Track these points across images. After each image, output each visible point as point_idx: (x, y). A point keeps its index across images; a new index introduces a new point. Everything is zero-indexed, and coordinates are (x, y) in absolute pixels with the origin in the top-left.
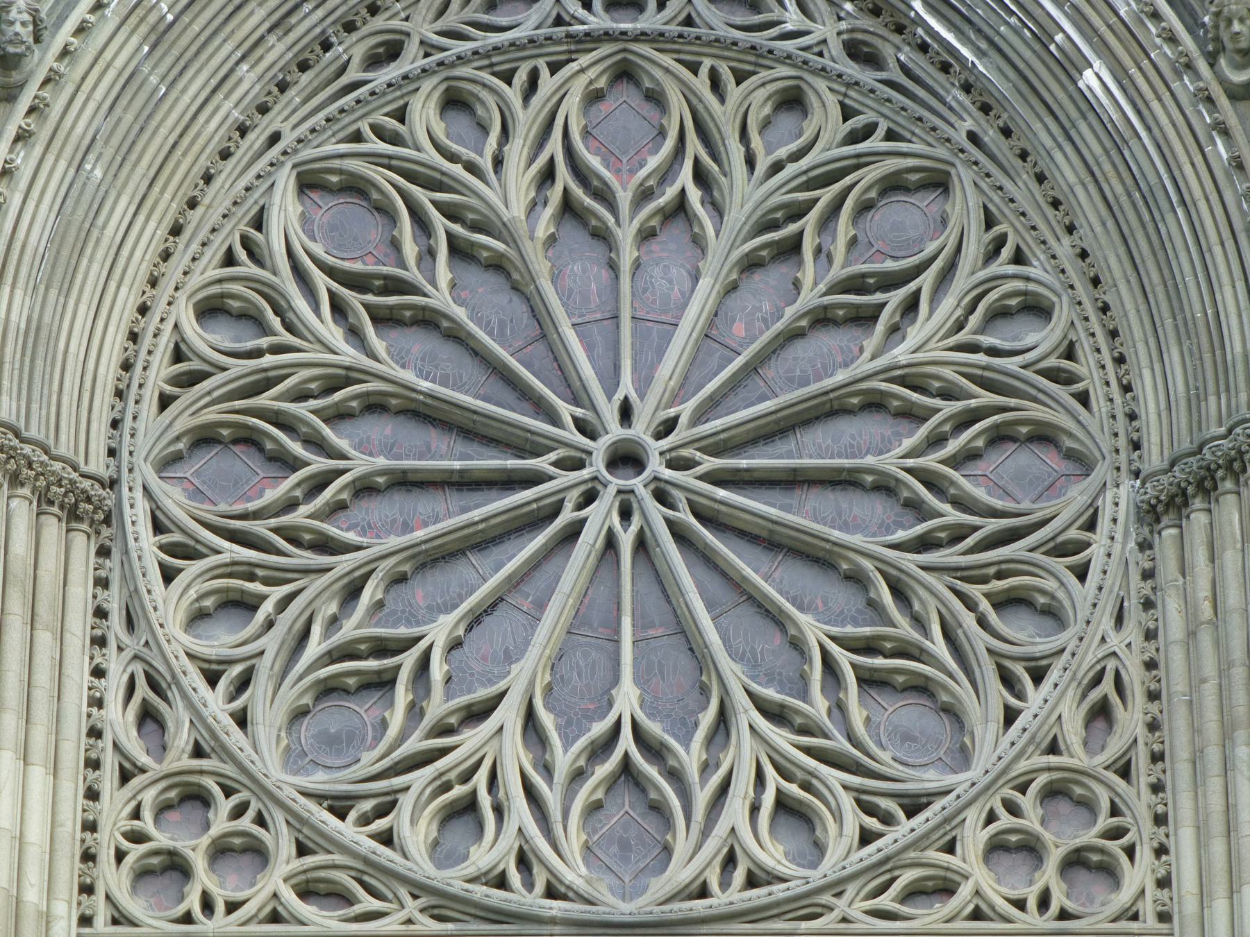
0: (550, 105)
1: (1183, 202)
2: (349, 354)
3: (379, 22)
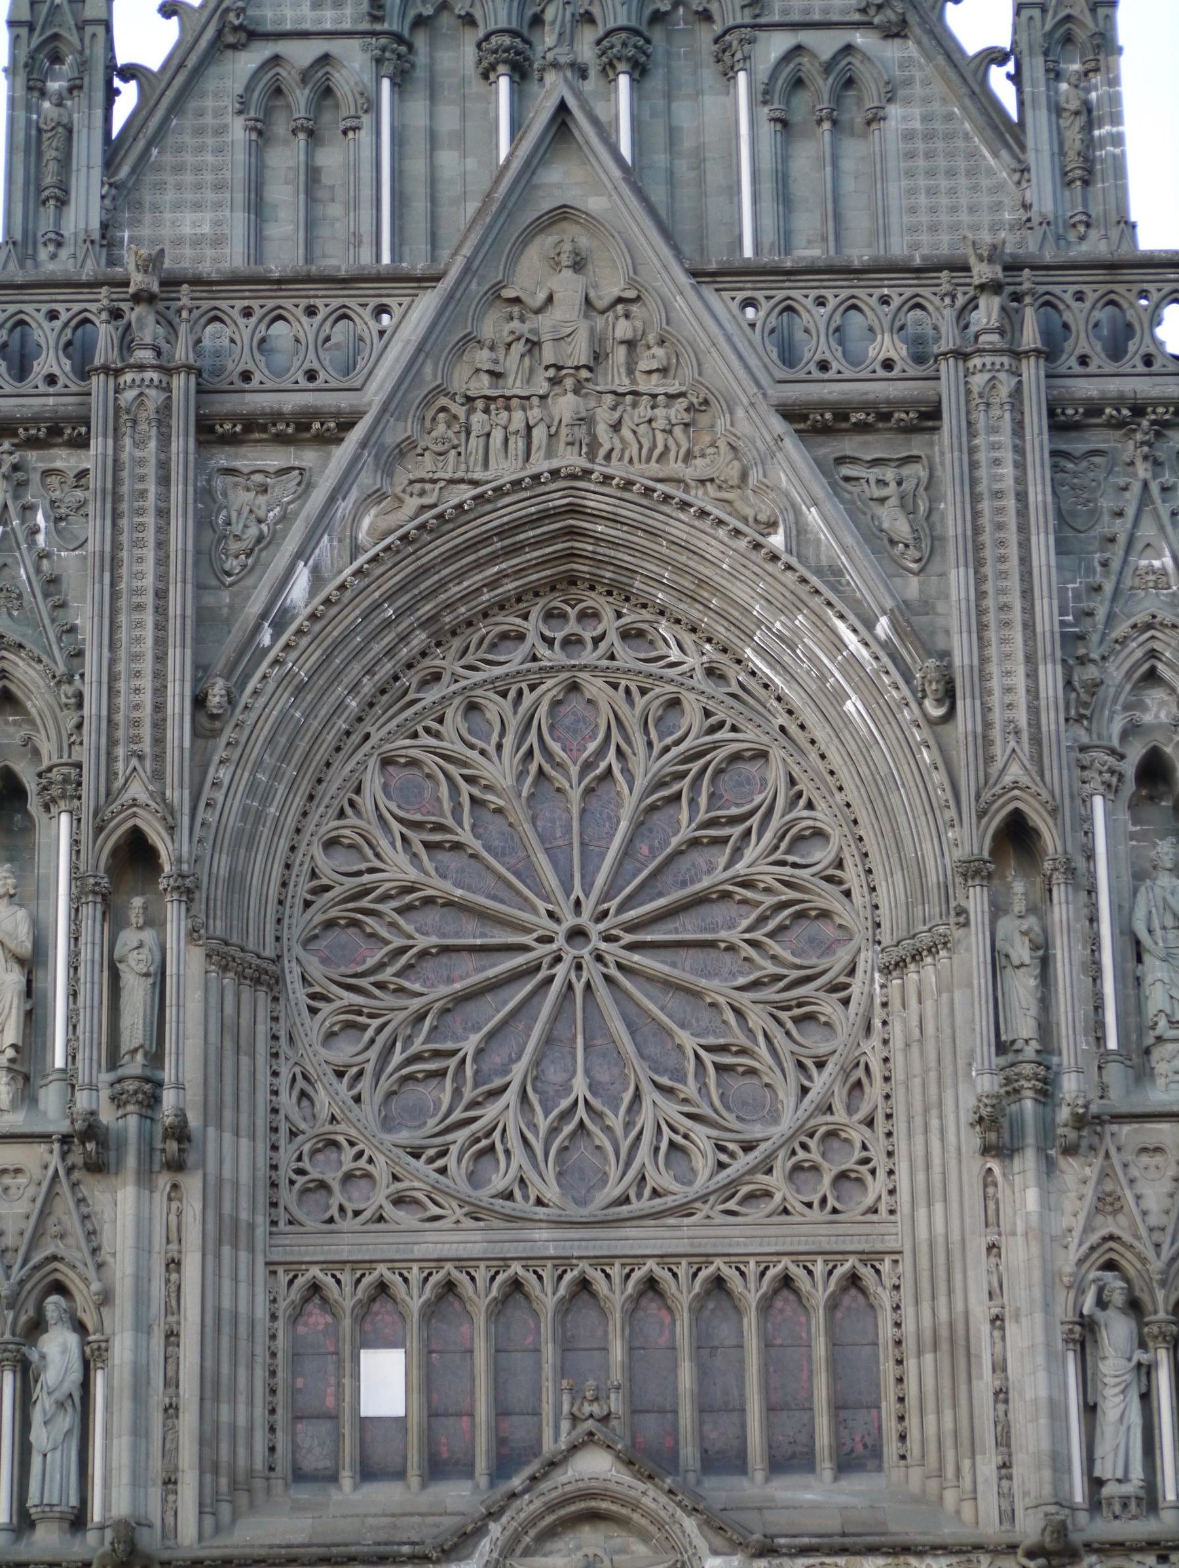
2: (413, 874)
3: (427, 662)
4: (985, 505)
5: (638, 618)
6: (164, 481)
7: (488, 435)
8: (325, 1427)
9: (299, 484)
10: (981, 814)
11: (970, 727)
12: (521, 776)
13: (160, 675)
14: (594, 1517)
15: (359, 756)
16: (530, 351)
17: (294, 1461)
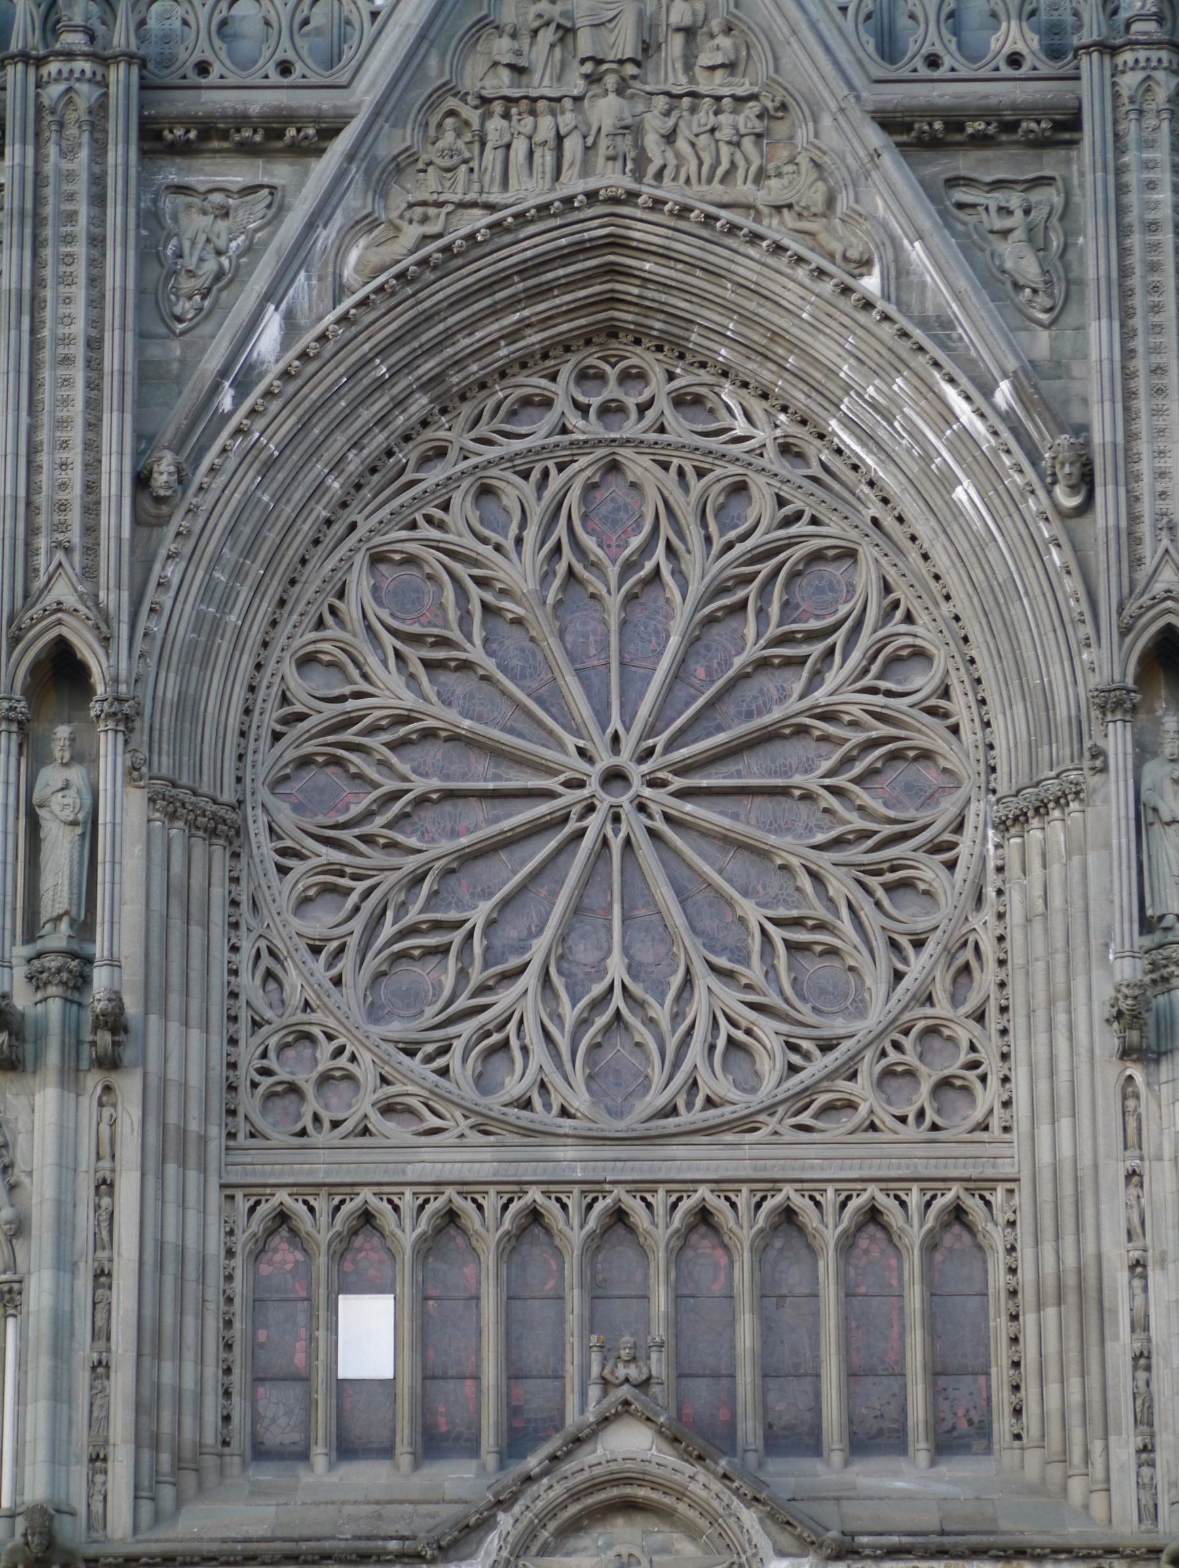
0: (558, 497)
1: (1027, 593)
2: (409, 700)
3: (429, 433)
4: (1135, 241)
5: (696, 380)
6: (99, 200)
7: (508, 146)
8: (293, 1392)
9: (269, 206)
10: (1125, 631)
11: (1111, 522)
12: (546, 578)
13: (92, 447)
14: (629, 1507)
15: (342, 551)
16: (562, 40)
17: (254, 1433)
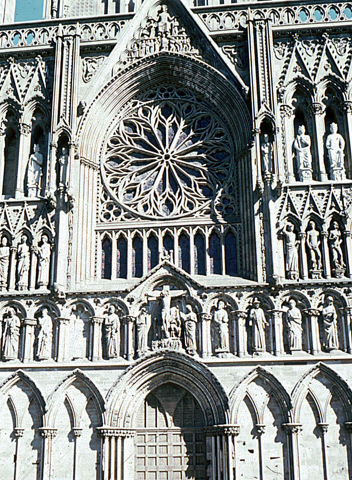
2: (130, 146)
